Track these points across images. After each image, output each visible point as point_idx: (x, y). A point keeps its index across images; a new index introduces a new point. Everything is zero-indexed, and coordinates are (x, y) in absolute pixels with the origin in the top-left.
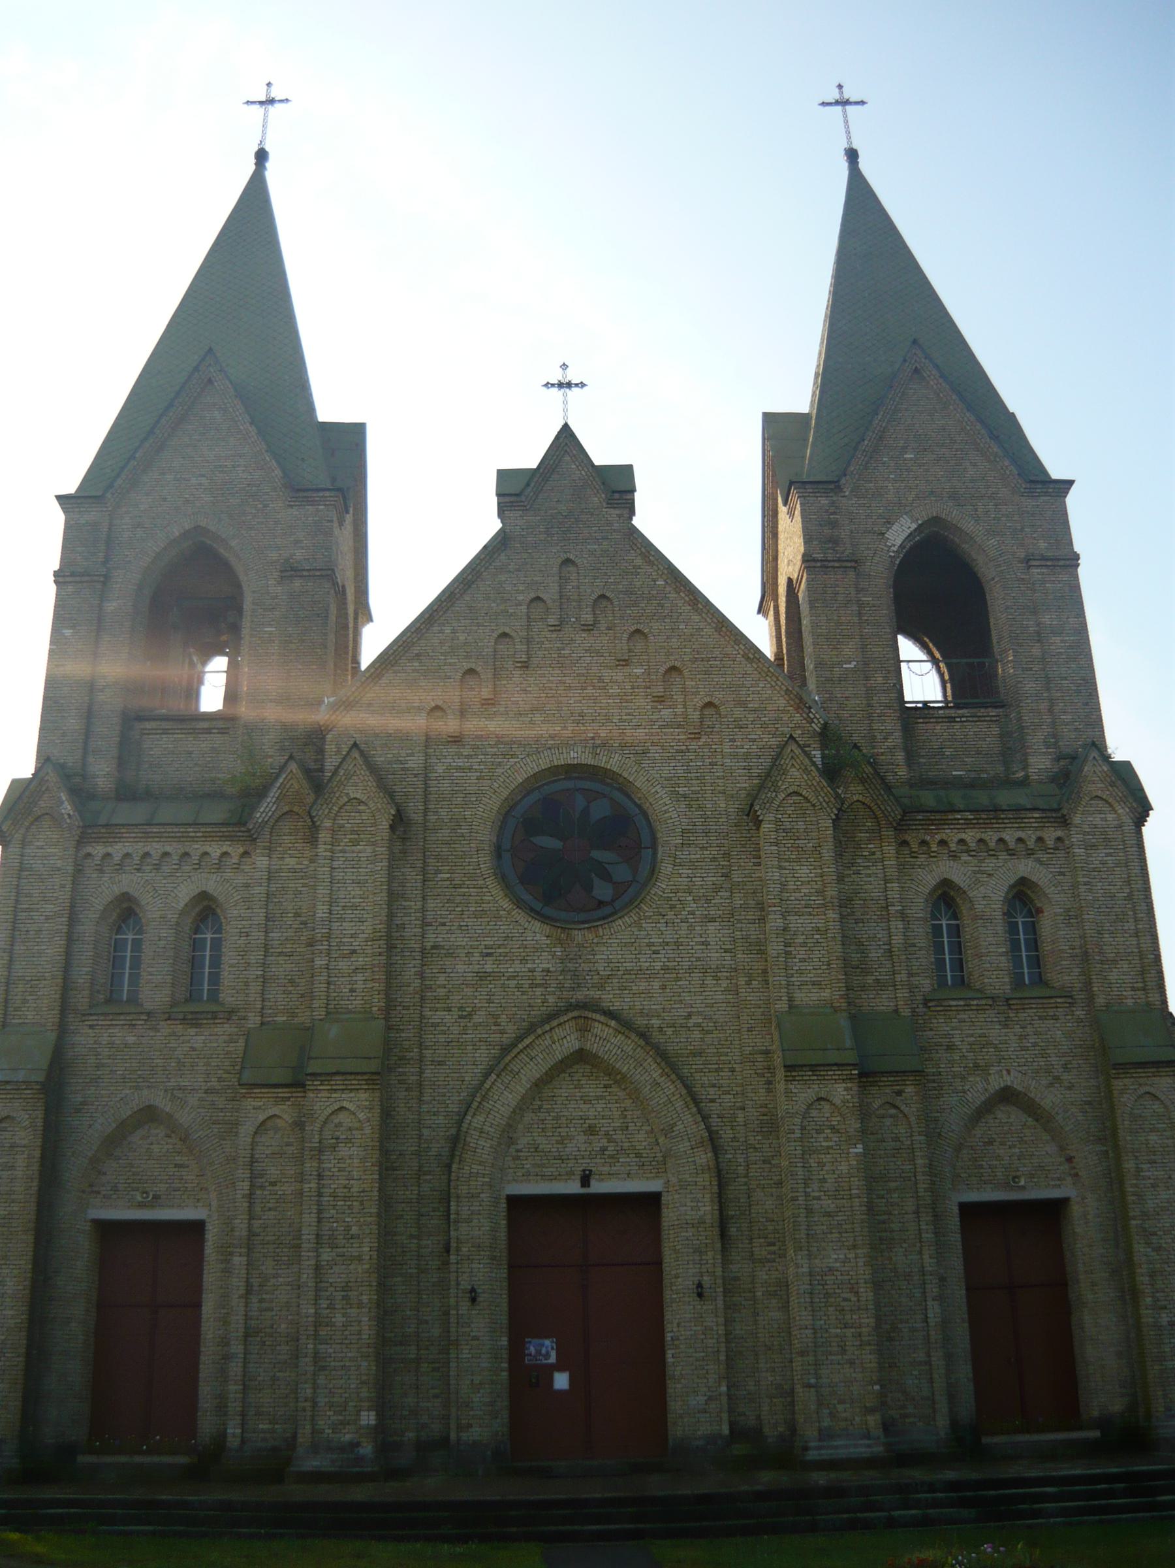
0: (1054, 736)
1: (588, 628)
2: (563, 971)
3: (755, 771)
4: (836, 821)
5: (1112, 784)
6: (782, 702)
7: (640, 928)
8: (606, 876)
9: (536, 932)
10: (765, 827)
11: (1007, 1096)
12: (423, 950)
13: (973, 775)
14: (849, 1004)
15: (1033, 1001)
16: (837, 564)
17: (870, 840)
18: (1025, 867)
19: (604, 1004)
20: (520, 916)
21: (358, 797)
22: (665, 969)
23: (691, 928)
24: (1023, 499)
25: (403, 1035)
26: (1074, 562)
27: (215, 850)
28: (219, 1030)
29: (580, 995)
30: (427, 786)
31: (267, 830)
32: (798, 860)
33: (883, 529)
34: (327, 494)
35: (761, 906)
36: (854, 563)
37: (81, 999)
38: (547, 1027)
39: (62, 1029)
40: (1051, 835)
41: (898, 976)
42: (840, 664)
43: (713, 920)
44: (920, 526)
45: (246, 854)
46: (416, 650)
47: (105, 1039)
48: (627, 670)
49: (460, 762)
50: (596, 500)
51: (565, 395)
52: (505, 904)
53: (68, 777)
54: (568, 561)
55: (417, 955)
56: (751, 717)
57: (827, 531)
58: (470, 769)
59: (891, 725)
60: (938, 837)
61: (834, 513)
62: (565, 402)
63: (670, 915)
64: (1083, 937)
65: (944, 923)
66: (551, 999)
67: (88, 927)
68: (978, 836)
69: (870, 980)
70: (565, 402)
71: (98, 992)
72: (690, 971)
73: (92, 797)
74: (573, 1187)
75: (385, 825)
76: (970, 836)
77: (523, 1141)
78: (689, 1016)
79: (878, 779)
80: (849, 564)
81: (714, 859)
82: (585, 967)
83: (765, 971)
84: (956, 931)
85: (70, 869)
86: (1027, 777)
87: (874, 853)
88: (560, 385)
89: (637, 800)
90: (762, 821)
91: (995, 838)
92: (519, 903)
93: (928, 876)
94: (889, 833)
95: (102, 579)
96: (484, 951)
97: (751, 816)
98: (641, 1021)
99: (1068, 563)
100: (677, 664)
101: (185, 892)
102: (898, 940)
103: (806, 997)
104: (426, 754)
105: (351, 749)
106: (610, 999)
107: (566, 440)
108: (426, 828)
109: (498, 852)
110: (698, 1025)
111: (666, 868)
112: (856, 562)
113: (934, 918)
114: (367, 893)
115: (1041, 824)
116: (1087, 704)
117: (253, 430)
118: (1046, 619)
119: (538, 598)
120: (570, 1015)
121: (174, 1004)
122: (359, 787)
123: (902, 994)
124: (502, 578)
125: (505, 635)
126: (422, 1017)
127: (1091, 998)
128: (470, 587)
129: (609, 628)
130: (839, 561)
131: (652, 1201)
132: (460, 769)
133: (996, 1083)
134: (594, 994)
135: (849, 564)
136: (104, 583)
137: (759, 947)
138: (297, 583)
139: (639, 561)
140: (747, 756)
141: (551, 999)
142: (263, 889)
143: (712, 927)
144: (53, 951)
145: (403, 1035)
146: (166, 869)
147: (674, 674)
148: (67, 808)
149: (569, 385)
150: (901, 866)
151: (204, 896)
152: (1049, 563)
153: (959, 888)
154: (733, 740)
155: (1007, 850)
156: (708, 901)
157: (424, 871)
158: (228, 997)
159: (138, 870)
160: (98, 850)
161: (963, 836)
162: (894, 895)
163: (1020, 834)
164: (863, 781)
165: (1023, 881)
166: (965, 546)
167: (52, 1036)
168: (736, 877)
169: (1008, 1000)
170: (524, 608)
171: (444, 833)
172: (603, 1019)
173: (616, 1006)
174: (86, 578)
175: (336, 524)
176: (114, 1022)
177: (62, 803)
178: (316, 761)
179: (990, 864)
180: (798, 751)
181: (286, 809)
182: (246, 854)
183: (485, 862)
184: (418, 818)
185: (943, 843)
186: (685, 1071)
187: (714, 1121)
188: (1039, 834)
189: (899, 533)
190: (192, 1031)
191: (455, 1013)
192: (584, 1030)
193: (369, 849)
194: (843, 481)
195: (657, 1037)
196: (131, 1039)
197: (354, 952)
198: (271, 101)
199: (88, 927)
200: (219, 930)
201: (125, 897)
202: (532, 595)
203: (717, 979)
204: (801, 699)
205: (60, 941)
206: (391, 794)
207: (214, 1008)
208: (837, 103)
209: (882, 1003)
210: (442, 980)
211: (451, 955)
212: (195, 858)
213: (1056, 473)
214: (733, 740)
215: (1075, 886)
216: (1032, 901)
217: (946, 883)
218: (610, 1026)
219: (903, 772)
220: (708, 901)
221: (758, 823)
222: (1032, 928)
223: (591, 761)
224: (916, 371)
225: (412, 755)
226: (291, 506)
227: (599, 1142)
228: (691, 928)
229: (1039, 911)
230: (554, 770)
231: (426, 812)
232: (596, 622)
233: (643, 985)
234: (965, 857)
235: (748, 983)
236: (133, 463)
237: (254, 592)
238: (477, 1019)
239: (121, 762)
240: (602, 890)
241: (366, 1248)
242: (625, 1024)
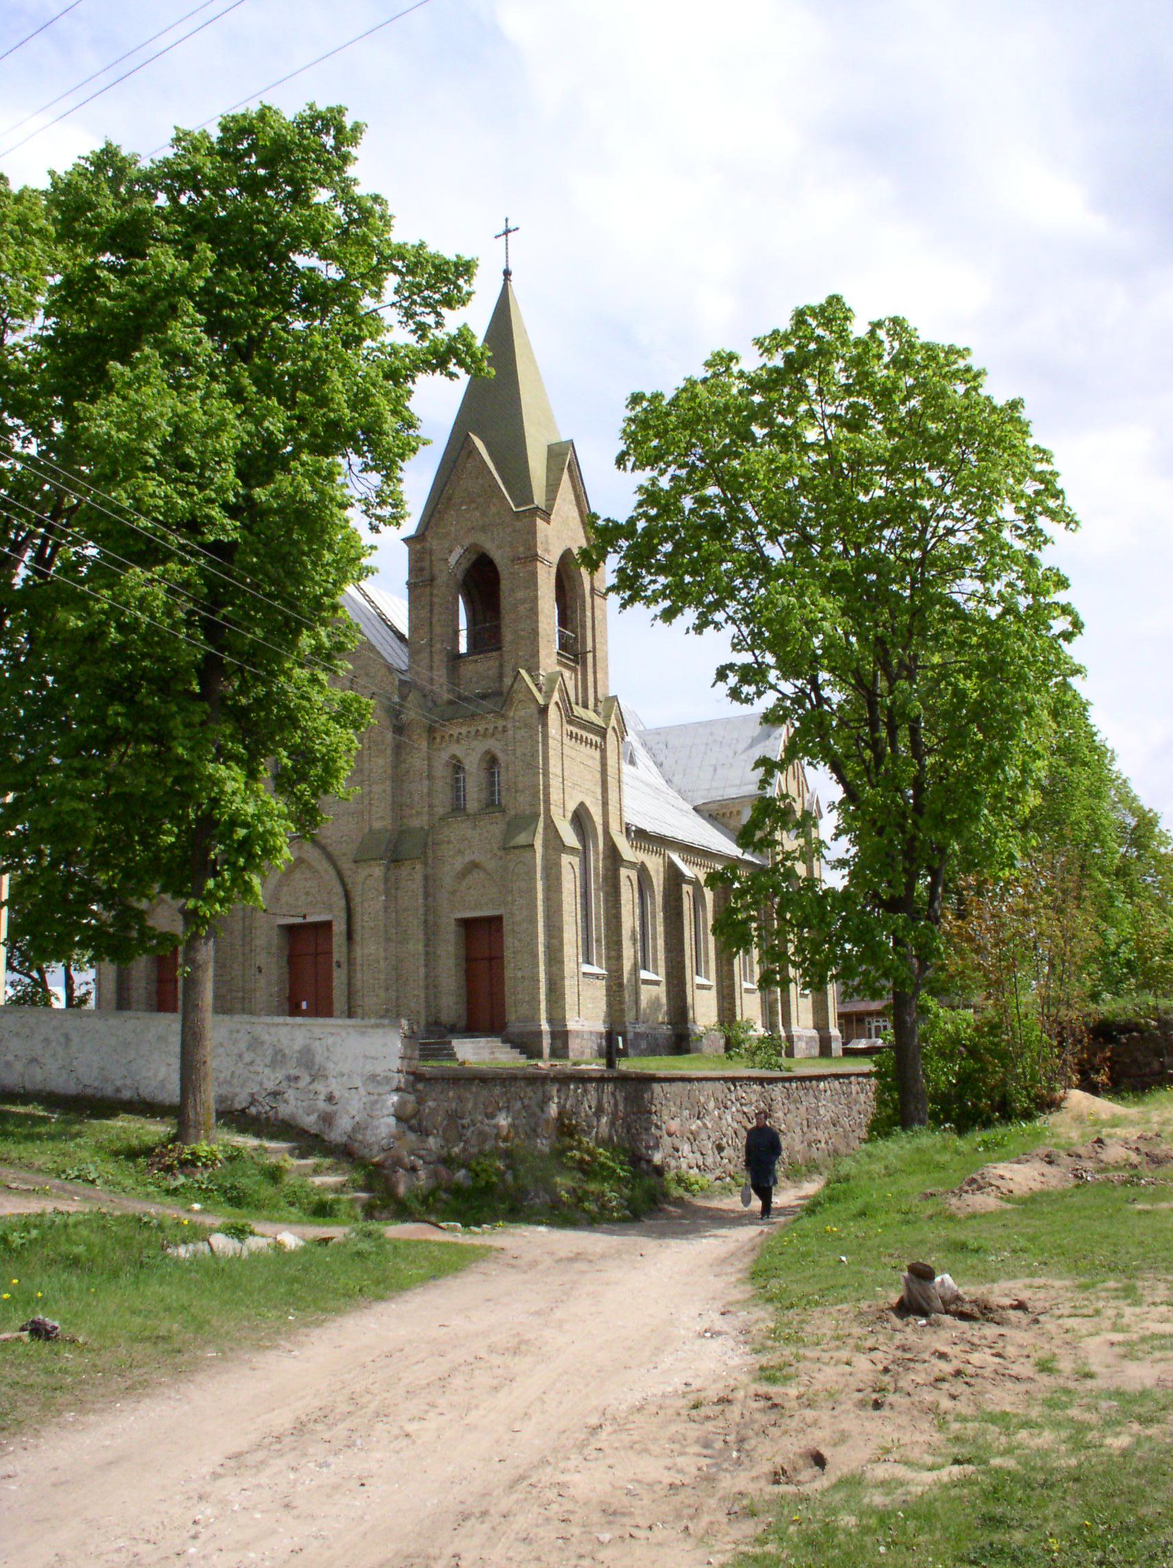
11: (474, 866)
74: (300, 920)
76: (464, 730)
77: (283, 900)
93: (444, 756)
103: (377, 825)
123: (425, 818)
131: (327, 925)
133: (467, 859)
192: (300, 848)
195: (330, 849)
209: (415, 823)
217: (454, 757)
227: (310, 899)
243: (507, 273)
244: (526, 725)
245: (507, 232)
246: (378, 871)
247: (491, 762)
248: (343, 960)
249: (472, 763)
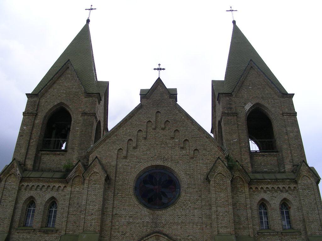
0: (292, 160)
1: (163, 129)
2: (152, 222)
3: (209, 168)
4: (231, 181)
5: (309, 172)
6: (216, 149)
7: (175, 210)
9: (145, 211)
10: (211, 182)
12: (112, 215)
13: (270, 170)
14: (235, 233)
15: (289, 233)
16: (232, 114)
17: (241, 187)
18: (285, 195)
19: (164, 232)
20: (141, 207)
21: (97, 171)
22: (182, 222)
23: (190, 211)
24: (281, 98)
25: (105, 239)
26: (295, 114)
27: (57, 185)
28: (53, 235)
29: (157, 229)
30: (116, 170)
31: (72, 180)
32: (221, 192)
33: (244, 106)
34: (95, 94)
35: (210, 205)
36: (236, 114)
37: (16, 225)
38: (147, 238)
39: (10, 233)
40: (292, 186)
41: (250, 226)
42: (232, 140)
43: (196, 209)
44: (253, 105)
45: (65, 187)
46: (116, 134)
47: (21, 236)
48: (173, 140)
49: (126, 164)
50: (166, 97)
51: (159, 71)
52: (137, 203)
53: (20, 165)
54: (158, 112)
55: (111, 216)
56: (208, 153)
57: (229, 106)
58: (129, 166)
59: (247, 157)
60: (260, 187)
61: (231, 101)
62: (159, 73)
63: (184, 207)
64: (303, 215)
65: (263, 211)
66: (149, 230)
67: (20, 205)
68: (272, 186)
69: (241, 226)
70: (159, 73)
71: (21, 223)
72: (189, 223)
73: (26, 170)
75: (104, 179)
78: (189, 236)
79: (243, 170)
80: (235, 114)
81: (197, 192)
82: (159, 221)
83: (211, 224)
84: (266, 214)
85: (17, 189)
86: (285, 171)
87: (242, 191)
88: (158, 69)
89: (175, 175)
90: (210, 181)
91: (277, 187)
92: (140, 203)
93: (258, 197)
94: (246, 185)
95: (35, 114)
96: (130, 216)
97: (208, 180)
99: (294, 114)
100: (187, 139)
101: (48, 196)
102: (249, 215)
104: (117, 161)
105: (95, 158)
106: (165, 230)
107: (159, 82)
108: (115, 181)
109: (135, 188)
110: (191, 239)
111: (183, 194)
112: (237, 113)
113: (260, 209)
114: (97, 198)
115: (290, 183)
116: (301, 151)
117: (78, 79)
118: (289, 129)
119: (150, 121)
120: (154, 235)
121: (42, 227)
122: (97, 169)
123: (251, 230)
124: (140, 116)
125: (140, 130)
126: (111, 234)
127: (306, 233)
128: (131, 118)
129: (169, 129)
130: (232, 113)
132: (125, 165)
134: (161, 229)
135: (235, 114)
136: (36, 116)
137: (209, 217)
138: (86, 116)
139: (177, 112)
140: (206, 164)
141: (149, 230)
142: (69, 196)
143: (196, 211)
144: (10, 211)
145: (105, 239)
146: (43, 190)
147: (187, 142)
148: (18, 172)
149: (161, 69)
150: (250, 195)
151: (53, 198)
152: (289, 114)
153: (266, 201)
154: (203, 159)
155: (280, 190)
156: (195, 203)
157: (114, 193)
158: (57, 226)
159: (36, 190)
160: (25, 184)
161: (268, 186)
162: (248, 202)
163: (284, 186)
164: (239, 171)
165: (285, 199)
166: (266, 111)
167: (6, 235)
168: (203, 197)
169: (282, 233)
170: (146, 124)
171: (120, 183)
172: (163, 236)
174: (31, 114)
175: (97, 103)
176: (24, 232)
177: (17, 171)
178: (87, 163)
179: (275, 194)
180: (221, 161)
181: (77, 175)
182: (65, 187)
183: (132, 192)
184: (113, 178)
188: (289, 186)
189: (248, 107)
190: (46, 235)
191: (121, 233)
193: (99, 186)
194: (233, 93)
196: (29, 237)
197: (92, 214)
198: (92, 9)
199: (20, 205)
200: (56, 208)
201: (32, 197)
202: (148, 120)
203: (197, 225)
204: (222, 148)
206: (106, 172)
207: (53, 229)
208: (230, 11)
209: (245, 233)
210: (117, 224)
211: (120, 217)
212: (51, 187)
213: (289, 92)
214: (203, 159)
215: (300, 200)
216: (288, 205)
218: (165, 238)
219: (250, 169)
220: (195, 203)
221: (209, 181)
222: (288, 213)
223: (162, 164)
224: (252, 67)
225: (113, 161)
226: (86, 98)
228: (190, 211)
229: (290, 208)
230: (152, 166)
231: (116, 177)
232: (165, 127)
233: (175, 227)
234: (268, 192)
235: (206, 227)
236: (46, 86)
237: (74, 119)
238: (127, 235)
239: (35, 162)
240: (165, 200)
244: (308, 188)
247: (285, 204)
249: (275, 202)
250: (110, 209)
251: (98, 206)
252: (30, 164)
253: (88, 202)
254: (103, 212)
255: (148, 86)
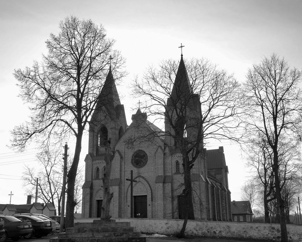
8: (143, 162)
37: (94, 178)
52: (132, 166)
69: (167, 172)
98: (145, 177)
103: (159, 175)
131: (146, 196)
160: (94, 162)
173: (143, 176)
184: (124, 156)
185: (176, 156)
186: (149, 182)
187: (152, 188)
192: (139, 179)
199: (94, 171)
205: (91, 172)
227: (141, 190)
241: (118, 202)
242: (143, 178)
243: (182, 55)
245: (182, 47)
246: (161, 185)
248: (151, 204)
250: (123, 169)
251: (119, 169)
252: (95, 153)
253: (116, 168)
254: (121, 170)
255: (135, 112)
